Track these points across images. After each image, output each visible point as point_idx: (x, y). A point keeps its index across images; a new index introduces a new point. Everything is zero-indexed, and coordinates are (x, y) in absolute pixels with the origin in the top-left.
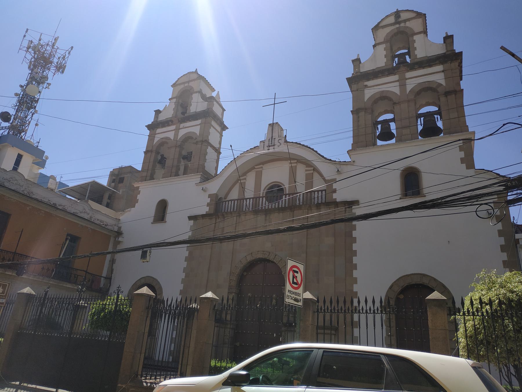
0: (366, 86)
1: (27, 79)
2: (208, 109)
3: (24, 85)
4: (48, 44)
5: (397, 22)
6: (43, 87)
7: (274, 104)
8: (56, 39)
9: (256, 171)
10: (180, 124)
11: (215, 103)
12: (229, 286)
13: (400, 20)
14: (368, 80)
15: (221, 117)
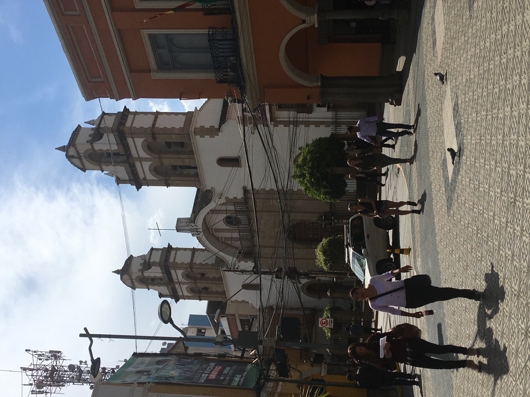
0: (145, 179)
1: (81, 385)
2: (160, 266)
3: (90, 385)
4: (31, 375)
5: (80, 158)
6: (87, 367)
7: (159, 229)
8: (25, 369)
9: (215, 232)
10: (174, 282)
11: (151, 261)
12: (306, 248)
13: (76, 155)
14: (138, 177)
15: (161, 251)
